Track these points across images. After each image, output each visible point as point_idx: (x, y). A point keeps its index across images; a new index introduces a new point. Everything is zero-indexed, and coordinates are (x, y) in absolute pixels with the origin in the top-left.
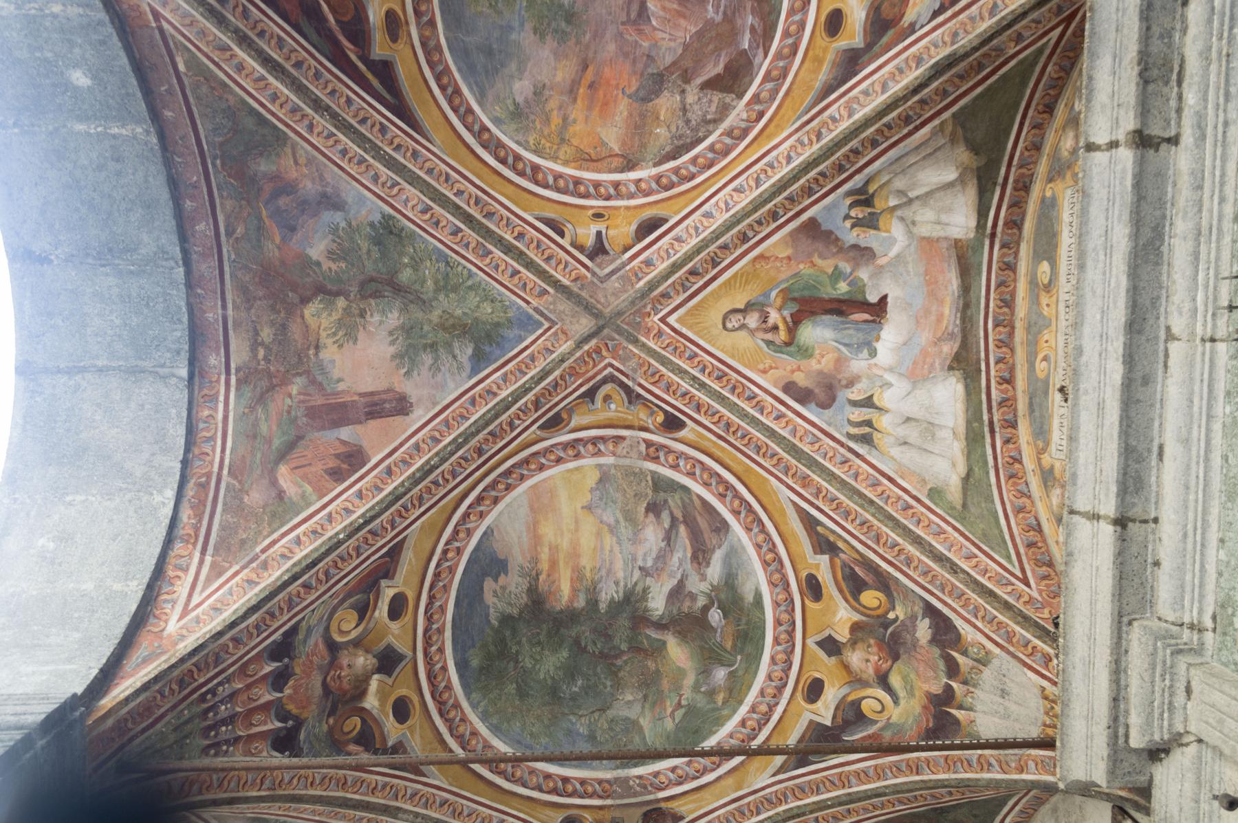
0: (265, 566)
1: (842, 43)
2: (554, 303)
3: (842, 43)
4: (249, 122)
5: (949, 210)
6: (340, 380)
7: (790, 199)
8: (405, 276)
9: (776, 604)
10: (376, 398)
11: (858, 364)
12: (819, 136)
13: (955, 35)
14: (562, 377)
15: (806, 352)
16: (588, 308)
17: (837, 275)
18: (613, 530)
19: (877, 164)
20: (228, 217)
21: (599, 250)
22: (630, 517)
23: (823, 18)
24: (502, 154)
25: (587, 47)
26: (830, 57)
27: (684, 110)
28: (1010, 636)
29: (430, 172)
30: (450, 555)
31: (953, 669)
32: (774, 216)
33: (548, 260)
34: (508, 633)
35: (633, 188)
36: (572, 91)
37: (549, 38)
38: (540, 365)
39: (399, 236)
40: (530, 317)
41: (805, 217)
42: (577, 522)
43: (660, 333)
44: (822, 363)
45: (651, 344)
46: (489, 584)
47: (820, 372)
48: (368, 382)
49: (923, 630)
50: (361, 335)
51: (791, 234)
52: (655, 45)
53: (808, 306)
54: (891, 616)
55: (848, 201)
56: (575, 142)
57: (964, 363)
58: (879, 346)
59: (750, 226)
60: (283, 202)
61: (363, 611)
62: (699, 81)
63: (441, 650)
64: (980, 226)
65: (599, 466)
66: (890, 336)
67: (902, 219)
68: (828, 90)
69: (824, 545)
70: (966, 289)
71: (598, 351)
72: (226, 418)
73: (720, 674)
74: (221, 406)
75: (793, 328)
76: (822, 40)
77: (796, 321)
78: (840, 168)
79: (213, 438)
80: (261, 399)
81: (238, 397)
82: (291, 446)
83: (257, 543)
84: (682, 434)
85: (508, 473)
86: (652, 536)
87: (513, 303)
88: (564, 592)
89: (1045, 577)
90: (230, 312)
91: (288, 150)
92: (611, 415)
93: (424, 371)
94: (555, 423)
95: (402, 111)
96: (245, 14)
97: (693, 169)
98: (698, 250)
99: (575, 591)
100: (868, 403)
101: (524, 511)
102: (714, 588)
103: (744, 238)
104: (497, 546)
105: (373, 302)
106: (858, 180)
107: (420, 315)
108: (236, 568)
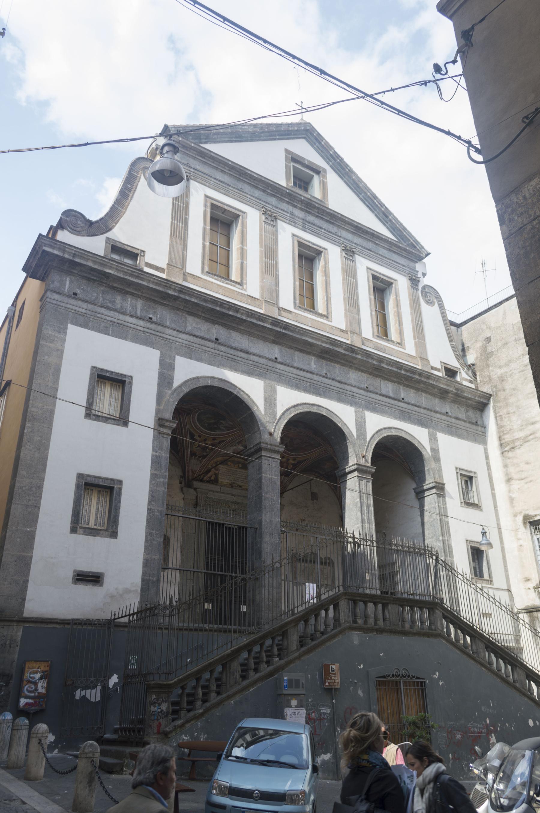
31: (199, 457)
49: (205, 454)
73: (206, 425)
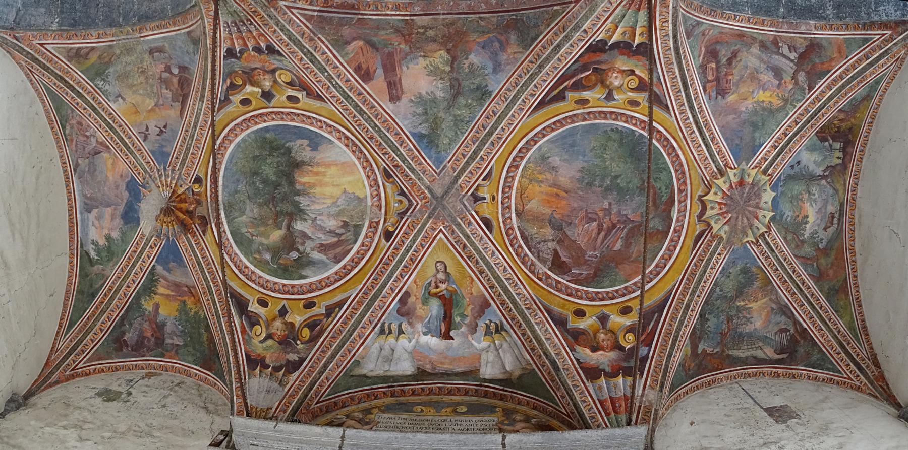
0: (311, 40)
1: (571, 317)
2: (449, 175)
3: (571, 317)
4: (533, 34)
5: (493, 367)
6: (408, 68)
7: (500, 295)
8: (462, 101)
9: (301, 286)
10: (398, 86)
11: (419, 327)
12: (528, 309)
13: (567, 370)
14: (411, 179)
15: (425, 302)
16: (446, 192)
17: (463, 316)
18: (334, 203)
19: (514, 335)
20: (488, 18)
21: (476, 198)
22: (341, 213)
23: (582, 308)
24: (524, 151)
25: (576, 193)
26: (565, 312)
27: (544, 242)
28: (292, 396)
29: (513, 116)
30: (319, 124)
32: (492, 287)
33: (471, 172)
34: (282, 151)
35: (507, 216)
36: (555, 185)
37: (580, 174)
38: (417, 168)
39: (481, 99)
40: (441, 163)
41: (491, 301)
42: (338, 185)
43: (434, 229)
44: (420, 310)
45: (428, 225)
46: (306, 142)
47: (415, 309)
48: (406, 83)
49: (293, 357)
50: (431, 78)
51: (483, 295)
52: (576, 226)
53: (449, 303)
54: (298, 342)
55: (498, 322)
56: (530, 187)
57: (421, 374)
58: (429, 336)
59: (487, 275)
60: (497, 44)
61: (291, 84)
62: (558, 248)
63: (273, 120)
64: (486, 380)
65: (366, 197)
66: (433, 341)
67: (489, 346)
68: (549, 312)
69: (330, 311)
70: (457, 375)
71: (425, 197)
72: (388, 15)
74: (394, 13)
75: (435, 295)
76: (573, 308)
77: (441, 297)
78: (513, 319)
79: (378, 10)
80: (397, 31)
81: (399, 20)
82: (373, 45)
83: (323, 35)
84: (383, 241)
85: (361, 152)
86: (332, 224)
87: (449, 154)
88: (303, 179)
89: (321, 410)
90: (442, 16)
91: (521, 50)
92: (392, 204)
93: (414, 109)
94: (387, 175)
95: (542, 104)
96: (580, 40)
97: (516, 246)
98: (476, 249)
99: (304, 184)
100: (401, 332)
101: (343, 160)
102: (308, 255)
103: (481, 272)
104: (324, 146)
105: (449, 83)
106: (508, 327)
107: (442, 107)
108: (311, 27)
